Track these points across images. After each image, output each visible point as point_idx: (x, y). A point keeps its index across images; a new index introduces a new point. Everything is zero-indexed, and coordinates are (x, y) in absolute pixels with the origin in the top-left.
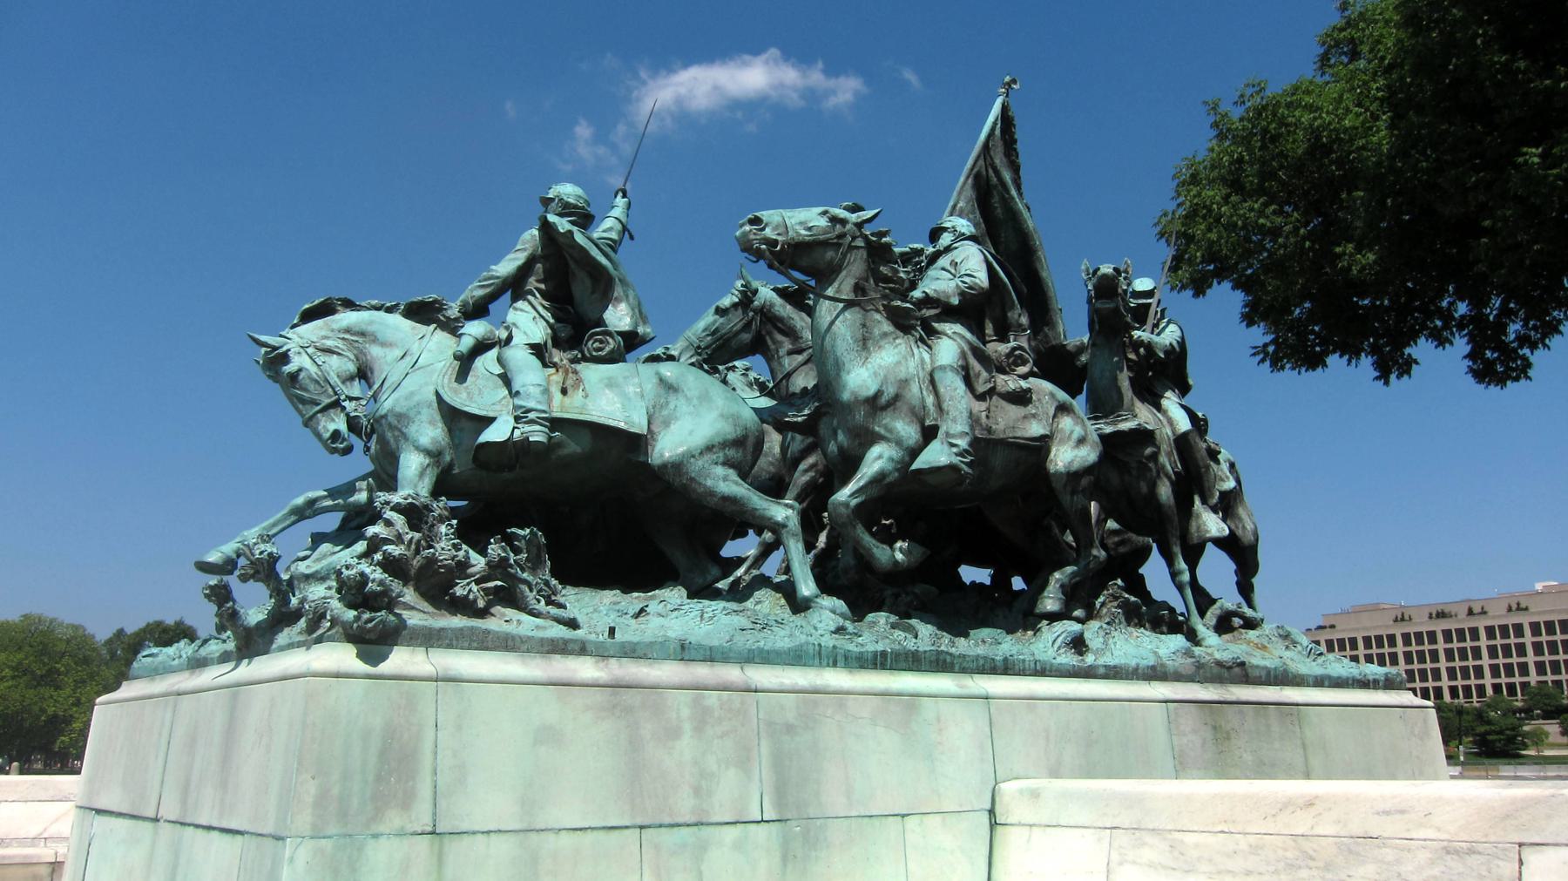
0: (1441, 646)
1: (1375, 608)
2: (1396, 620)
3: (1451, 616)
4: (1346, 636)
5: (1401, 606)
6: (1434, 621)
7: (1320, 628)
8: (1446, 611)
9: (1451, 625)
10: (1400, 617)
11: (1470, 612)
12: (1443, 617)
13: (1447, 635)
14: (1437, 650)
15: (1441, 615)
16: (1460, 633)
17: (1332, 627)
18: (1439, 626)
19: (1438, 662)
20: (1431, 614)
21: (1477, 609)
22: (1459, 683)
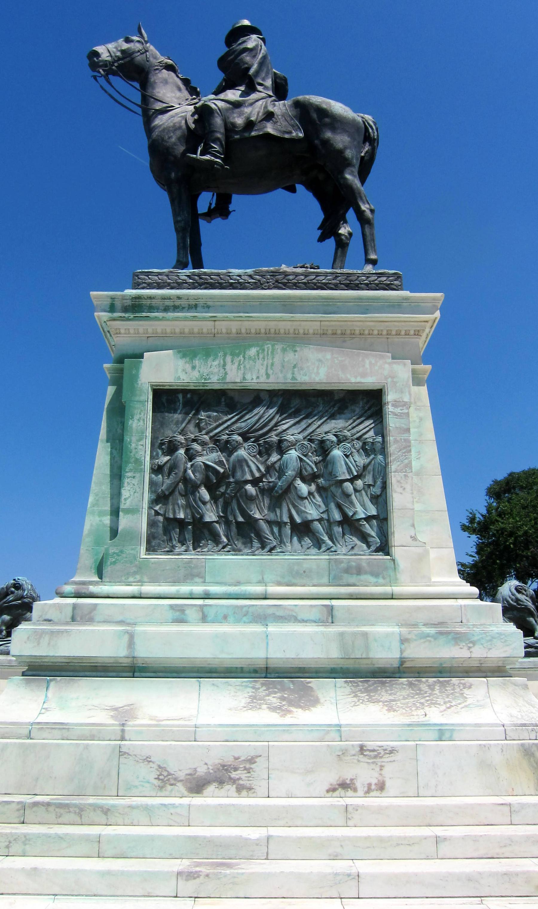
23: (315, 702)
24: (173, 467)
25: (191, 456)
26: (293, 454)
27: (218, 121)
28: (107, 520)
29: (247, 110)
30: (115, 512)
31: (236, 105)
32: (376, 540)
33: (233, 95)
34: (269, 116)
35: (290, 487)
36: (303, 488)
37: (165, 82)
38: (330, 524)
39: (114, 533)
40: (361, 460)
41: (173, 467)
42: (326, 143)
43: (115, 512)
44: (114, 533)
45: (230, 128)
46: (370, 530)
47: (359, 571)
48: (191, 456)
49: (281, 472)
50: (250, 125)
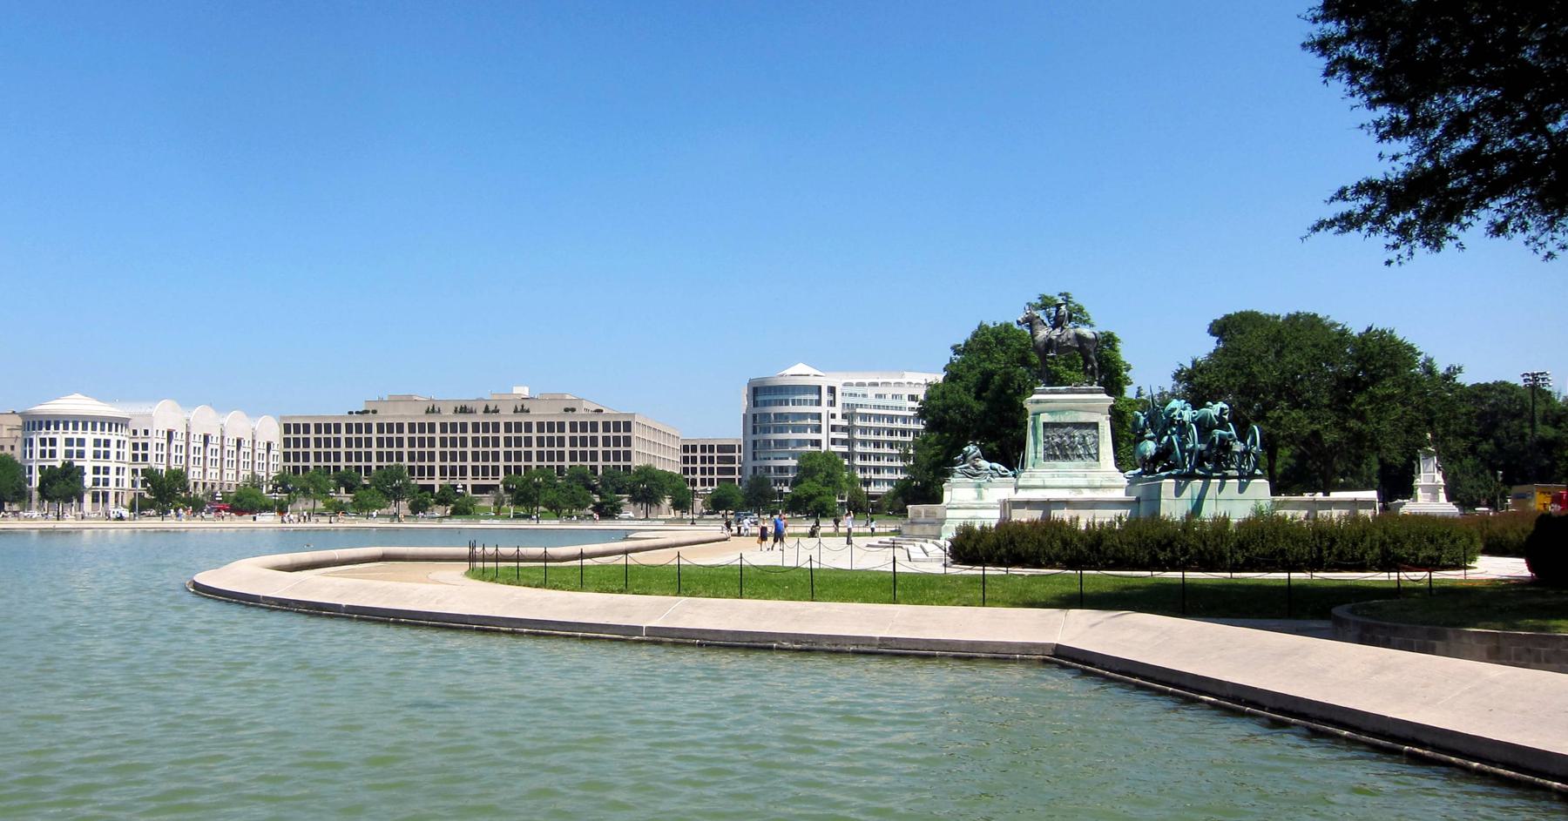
0: (470, 435)
1: (409, 399)
2: (427, 412)
3: (471, 412)
4: (395, 421)
5: (431, 400)
6: (458, 414)
7: (366, 412)
8: (469, 406)
9: (480, 418)
10: (431, 408)
11: (487, 410)
12: (465, 412)
13: (476, 427)
14: (434, 438)
15: (464, 410)
16: (486, 425)
17: (374, 412)
18: (469, 420)
19: (466, 446)
20: (456, 408)
21: (491, 408)
22: (448, 464)
23: (1082, 493)
24: (1048, 442)
25: (1053, 439)
26: (1077, 438)
27: (1055, 343)
28: (1034, 454)
29: (1062, 337)
30: (1036, 453)
31: (1059, 336)
32: (1096, 458)
33: (1058, 331)
34: (1069, 339)
35: (1076, 446)
36: (1079, 446)
37: (1037, 323)
38: (1085, 455)
39: (1036, 457)
40: (1092, 440)
41: (1048, 442)
42: (1085, 347)
43: (1036, 453)
44: (1036, 457)
45: (1058, 343)
46: (1095, 456)
47: (1092, 466)
48: (1053, 439)
49: (1074, 443)
50: (1063, 343)
